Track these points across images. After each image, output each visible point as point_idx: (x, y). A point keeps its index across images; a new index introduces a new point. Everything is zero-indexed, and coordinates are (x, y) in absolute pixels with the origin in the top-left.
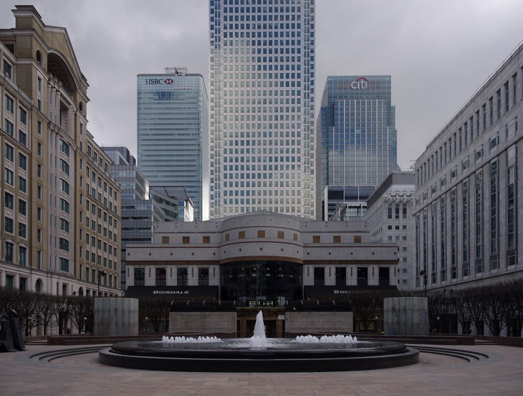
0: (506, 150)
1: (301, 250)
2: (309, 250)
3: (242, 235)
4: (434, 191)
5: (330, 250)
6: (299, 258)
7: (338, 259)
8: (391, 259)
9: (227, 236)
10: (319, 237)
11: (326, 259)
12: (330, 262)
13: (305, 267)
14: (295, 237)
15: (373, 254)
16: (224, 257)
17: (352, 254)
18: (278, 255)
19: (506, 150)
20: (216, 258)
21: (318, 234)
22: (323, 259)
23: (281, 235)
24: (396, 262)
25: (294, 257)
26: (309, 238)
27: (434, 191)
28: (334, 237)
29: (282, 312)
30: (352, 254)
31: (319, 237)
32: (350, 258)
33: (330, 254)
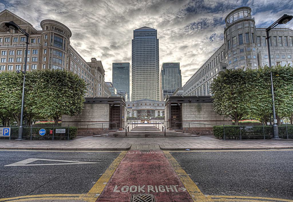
0: (211, 79)
1: (154, 107)
2: (156, 107)
3: (141, 104)
4: (187, 93)
5: (161, 107)
9: (138, 105)
13: (156, 111)
14: (153, 105)
16: (138, 109)
19: (211, 79)
20: (136, 109)
23: (150, 104)
27: (187, 93)
29: (150, 120)
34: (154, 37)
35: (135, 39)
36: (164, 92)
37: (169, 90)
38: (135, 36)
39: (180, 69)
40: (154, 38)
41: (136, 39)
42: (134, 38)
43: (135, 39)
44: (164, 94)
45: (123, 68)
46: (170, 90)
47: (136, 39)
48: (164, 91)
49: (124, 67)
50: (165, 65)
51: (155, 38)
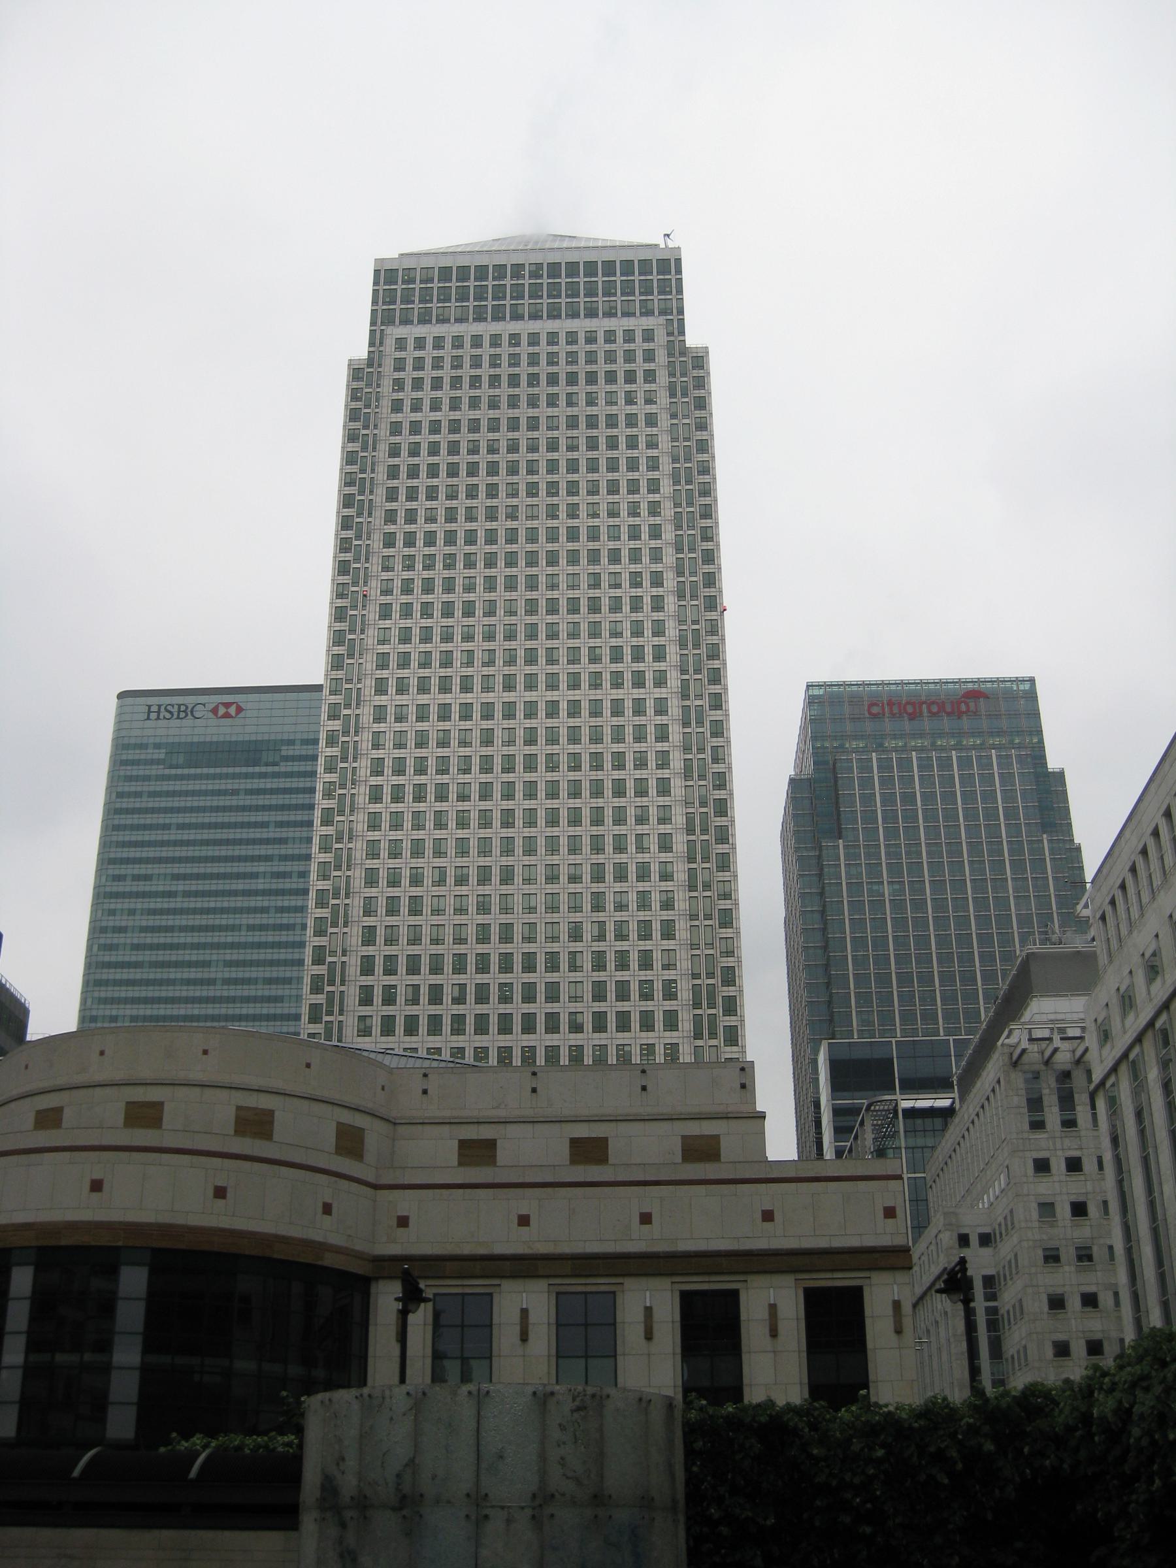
2: (405, 1203)
6: (336, 1239)
7: (566, 1249)
8: (869, 1241)
10: (491, 1144)
11: (499, 1249)
12: (524, 1266)
13: (386, 1298)
14: (350, 1142)
15: (768, 1216)
17: (646, 1219)
18: (194, 1221)
21: (486, 1133)
22: (482, 1251)
24: (894, 1259)
25: (295, 1232)
26: (436, 1153)
28: (575, 1143)
30: (646, 1219)
31: (491, 1144)
32: (639, 1241)
33: (524, 1221)
34: (639, 323)
35: (390, 343)
36: (837, 1086)
37: (910, 1050)
38: (388, 320)
39: (1053, 763)
40: (648, 336)
41: (401, 344)
42: (375, 339)
43: (390, 345)
44: (837, 1112)
45: (251, 753)
46: (938, 1051)
47: (401, 344)
48: (837, 1068)
49: (273, 746)
50: (850, 725)
51: (661, 337)
